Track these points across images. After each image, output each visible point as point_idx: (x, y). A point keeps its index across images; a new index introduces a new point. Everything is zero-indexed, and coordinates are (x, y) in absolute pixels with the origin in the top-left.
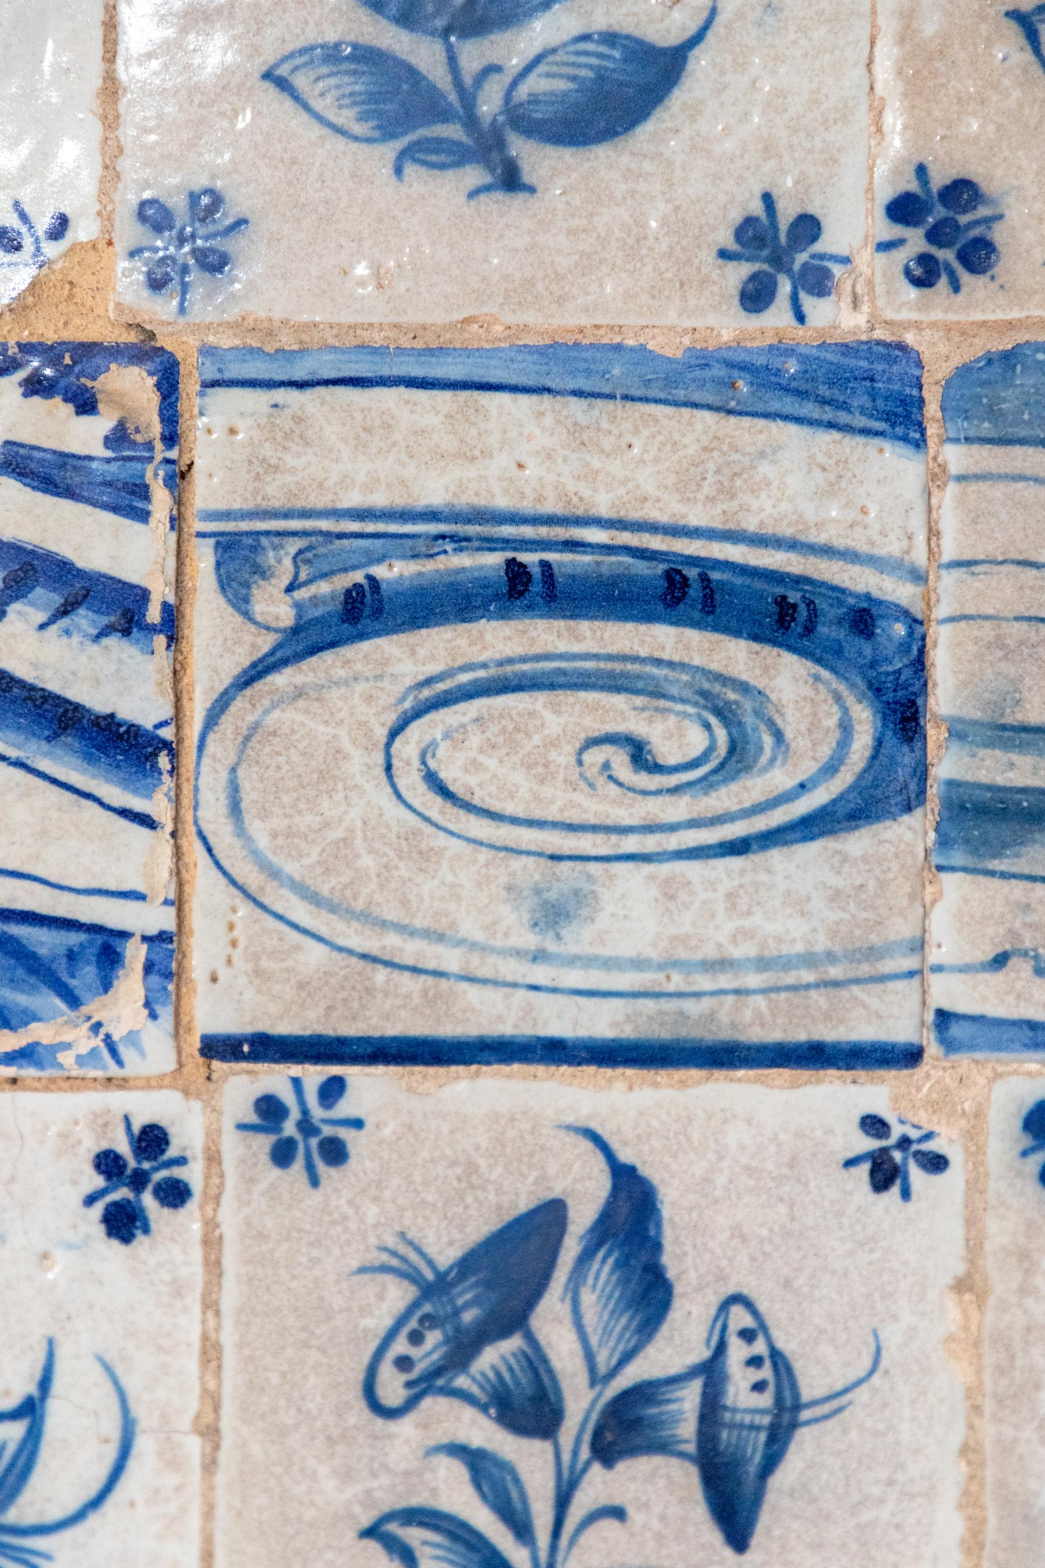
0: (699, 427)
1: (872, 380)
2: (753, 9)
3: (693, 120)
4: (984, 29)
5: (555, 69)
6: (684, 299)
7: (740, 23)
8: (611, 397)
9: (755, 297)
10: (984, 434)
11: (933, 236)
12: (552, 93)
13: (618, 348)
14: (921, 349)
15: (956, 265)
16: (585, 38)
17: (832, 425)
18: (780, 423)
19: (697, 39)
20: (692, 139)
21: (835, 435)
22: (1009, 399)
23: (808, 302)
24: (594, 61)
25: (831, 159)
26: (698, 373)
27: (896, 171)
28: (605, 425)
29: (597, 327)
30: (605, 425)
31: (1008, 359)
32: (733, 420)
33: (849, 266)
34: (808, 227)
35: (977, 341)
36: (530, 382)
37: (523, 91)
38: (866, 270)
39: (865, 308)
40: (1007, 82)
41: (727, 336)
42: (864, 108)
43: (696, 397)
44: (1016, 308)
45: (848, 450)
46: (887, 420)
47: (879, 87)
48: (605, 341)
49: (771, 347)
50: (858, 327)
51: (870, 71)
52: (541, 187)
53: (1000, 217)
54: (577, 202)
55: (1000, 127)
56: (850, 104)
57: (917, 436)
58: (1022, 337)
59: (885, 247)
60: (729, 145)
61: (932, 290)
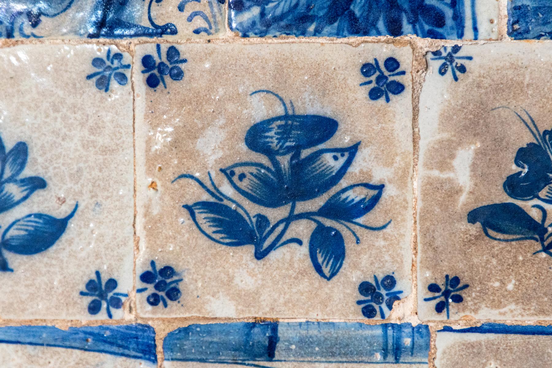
0: (74, 356)
1: (137, 338)
2: (91, 205)
3: (70, 245)
4: (175, 212)
5: (19, 227)
6: (68, 310)
7: (86, 210)
8: (42, 345)
9: (94, 309)
10: (178, 357)
11: (157, 287)
12: (18, 236)
13: (44, 327)
14: (154, 327)
15: (165, 297)
16: (30, 216)
17: (122, 355)
18: (104, 354)
19: (71, 216)
20: (69, 252)
21: (124, 358)
22: (187, 345)
23: (113, 310)
24: (34, 224)
25: (120, 259)
26: (74, 336)
27: (144, 264)
28: (40, 355)
29: (36, 320)
30: (40, 355)
31: (186, 330)
32: (87, 353)
33: (127, 298)
34: (112, 283)
35: (174, 324)
36: (13, 339)
37: (8, 235)
38: (134, 299)
39: (134, 312)
40: (183, 231)
41: (84, 323)
42: (132, 240)
43: (74, 344)
44: (187, 313)
45: (128, 364)
46: (142, 353)
47: (137, 233)
48: (40, 325)
49: (100, 327)
50: (131, 319)
51: (134, 227)
52: (15, 269)
53: (181, 280)
54: (28, 275)
55: (181, 247)
56: (127, 239)
57: (153, 358)
58: (191, 323)
59: (139, 291)
60: (83, 254)
61: (157, 307)
